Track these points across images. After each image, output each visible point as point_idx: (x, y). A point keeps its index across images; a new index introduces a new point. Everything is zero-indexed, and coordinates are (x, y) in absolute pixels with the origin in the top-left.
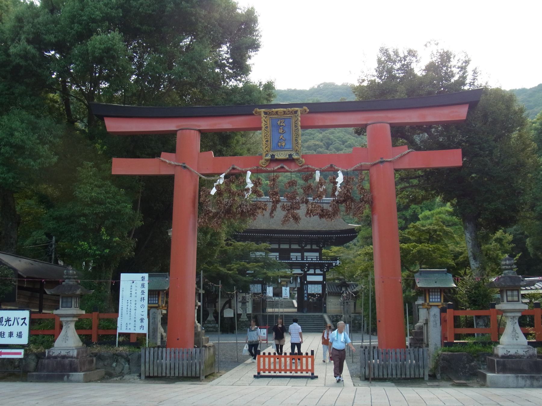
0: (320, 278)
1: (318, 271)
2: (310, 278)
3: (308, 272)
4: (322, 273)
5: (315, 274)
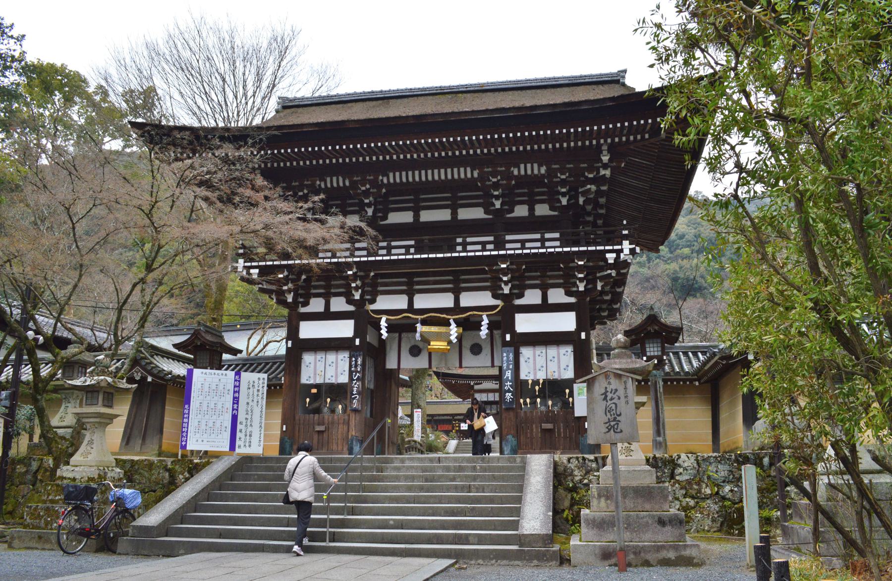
0: (566, 322)
1: (557, 296)
2: (525, 323)
3: (518, 302)
4: (572, 300)
5: (545, 307)
